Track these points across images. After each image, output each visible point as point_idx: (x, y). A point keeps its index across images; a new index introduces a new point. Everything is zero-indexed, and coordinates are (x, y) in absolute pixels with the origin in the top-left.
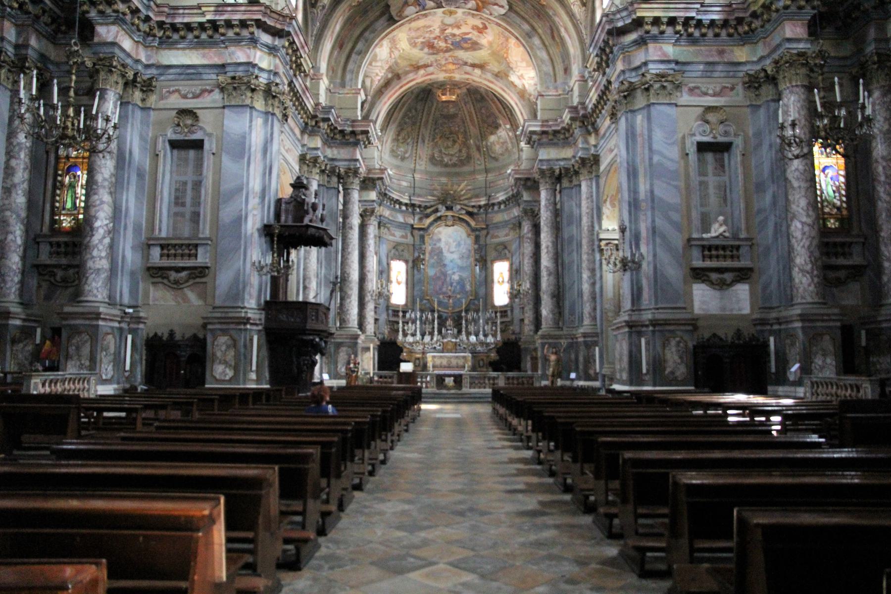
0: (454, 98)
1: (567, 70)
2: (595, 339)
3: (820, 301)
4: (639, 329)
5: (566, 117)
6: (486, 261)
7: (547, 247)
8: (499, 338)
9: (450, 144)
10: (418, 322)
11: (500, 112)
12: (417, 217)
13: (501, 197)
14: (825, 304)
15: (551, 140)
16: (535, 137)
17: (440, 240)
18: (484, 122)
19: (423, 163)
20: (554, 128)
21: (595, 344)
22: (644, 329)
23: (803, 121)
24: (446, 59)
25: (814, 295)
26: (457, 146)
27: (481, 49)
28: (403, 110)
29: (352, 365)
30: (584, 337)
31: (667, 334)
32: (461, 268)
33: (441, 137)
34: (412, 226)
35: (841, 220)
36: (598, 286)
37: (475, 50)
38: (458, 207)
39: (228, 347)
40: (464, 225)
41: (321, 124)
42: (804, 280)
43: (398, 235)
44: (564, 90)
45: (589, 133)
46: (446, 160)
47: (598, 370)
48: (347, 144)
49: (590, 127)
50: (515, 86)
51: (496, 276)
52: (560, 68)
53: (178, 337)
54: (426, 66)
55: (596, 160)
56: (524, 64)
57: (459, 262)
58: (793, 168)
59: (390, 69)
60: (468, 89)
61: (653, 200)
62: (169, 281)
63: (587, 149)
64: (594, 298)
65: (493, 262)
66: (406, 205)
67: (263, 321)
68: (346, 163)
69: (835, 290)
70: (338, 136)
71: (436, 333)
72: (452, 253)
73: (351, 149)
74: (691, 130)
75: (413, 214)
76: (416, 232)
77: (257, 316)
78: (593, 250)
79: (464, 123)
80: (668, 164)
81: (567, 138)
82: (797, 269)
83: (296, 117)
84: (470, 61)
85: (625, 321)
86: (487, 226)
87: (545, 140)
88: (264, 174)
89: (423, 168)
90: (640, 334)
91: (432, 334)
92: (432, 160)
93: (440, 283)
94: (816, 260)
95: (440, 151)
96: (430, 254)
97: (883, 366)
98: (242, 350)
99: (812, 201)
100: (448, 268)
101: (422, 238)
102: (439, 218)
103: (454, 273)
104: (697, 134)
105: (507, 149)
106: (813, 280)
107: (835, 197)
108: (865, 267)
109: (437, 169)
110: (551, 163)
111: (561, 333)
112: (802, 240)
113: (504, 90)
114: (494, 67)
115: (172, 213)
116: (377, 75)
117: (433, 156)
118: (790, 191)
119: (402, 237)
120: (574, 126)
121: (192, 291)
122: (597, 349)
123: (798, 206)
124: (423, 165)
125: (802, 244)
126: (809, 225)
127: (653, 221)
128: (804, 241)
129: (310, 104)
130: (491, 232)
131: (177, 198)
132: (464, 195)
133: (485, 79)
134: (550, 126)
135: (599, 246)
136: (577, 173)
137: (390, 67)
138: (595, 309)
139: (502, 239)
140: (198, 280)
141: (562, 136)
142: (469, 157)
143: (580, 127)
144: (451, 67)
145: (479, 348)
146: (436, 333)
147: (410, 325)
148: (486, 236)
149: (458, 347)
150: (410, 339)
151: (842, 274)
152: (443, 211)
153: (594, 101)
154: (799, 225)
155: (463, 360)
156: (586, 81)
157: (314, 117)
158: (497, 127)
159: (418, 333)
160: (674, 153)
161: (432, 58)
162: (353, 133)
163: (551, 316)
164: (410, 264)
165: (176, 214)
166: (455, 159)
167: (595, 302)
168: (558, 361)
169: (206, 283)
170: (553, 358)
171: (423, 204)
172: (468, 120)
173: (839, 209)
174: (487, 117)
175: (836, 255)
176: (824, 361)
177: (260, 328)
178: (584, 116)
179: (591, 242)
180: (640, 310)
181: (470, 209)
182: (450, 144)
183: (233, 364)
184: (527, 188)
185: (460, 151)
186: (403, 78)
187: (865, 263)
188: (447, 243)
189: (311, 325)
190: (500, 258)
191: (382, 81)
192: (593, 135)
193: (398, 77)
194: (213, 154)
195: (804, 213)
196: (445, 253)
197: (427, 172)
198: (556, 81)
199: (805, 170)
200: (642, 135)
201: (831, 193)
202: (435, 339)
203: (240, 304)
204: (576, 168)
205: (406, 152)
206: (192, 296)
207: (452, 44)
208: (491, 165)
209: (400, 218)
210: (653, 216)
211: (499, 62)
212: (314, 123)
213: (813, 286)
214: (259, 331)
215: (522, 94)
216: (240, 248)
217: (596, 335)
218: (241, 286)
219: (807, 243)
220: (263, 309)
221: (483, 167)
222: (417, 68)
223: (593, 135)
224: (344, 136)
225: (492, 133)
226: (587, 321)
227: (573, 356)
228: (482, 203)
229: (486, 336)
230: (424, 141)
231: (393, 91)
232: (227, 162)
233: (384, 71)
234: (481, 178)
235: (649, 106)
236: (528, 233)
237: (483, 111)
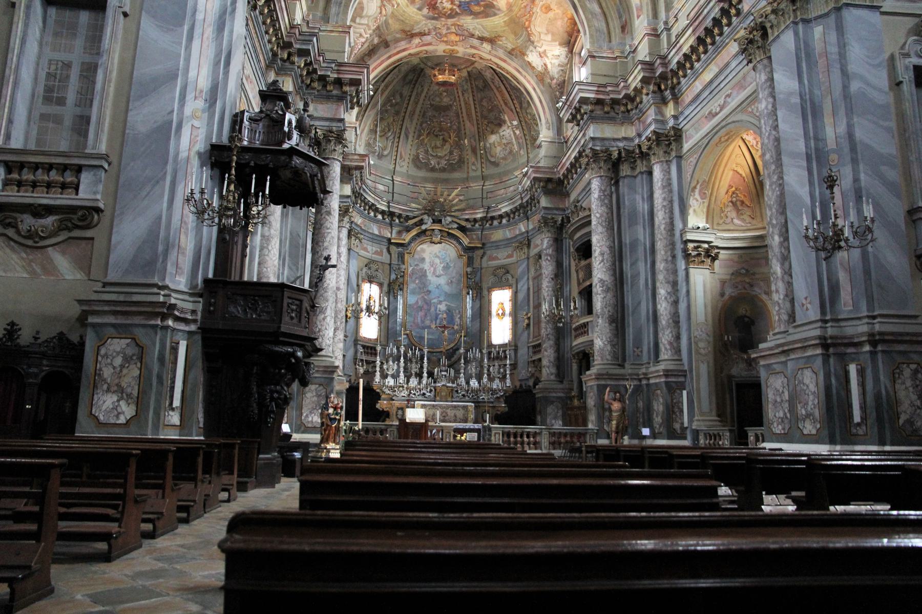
0: (453, 79)
1: (626, 27)
2: (682, 379)
4: (842, 349)
5: (635, 79)
6: (481, 288)
7: (602, 254)
8: (508, 383)
9: (439, 143)
10: (402, 360)
11: (506, 104)
12: (395, 230)
13: (505, 208)
15: (608, 113)
16: (585, 108)
17: (423, 260)
18: (485, 118)
19: (405, 164)
20: (612, 96)
21: (682, 386)
22: (851, 350)
24: (448, 29)
26: (447, 147)
27: (495, 15)
28: (386, 93)
29: (331, 411)
30: (666, 376)
31: (899, 359)
32: (448, 296)
33: (428, 134)
34: (389, 240)
36: (682, 306)
37: (487, 15)
38: (449, 219)
39: (127, 360)
40: (455, 242)
41: (296, 59)
43: (370, 250)
44: (622, 52)
45: (664, 102)
46: (432, 162)
47: (686, 425)
48: (328, 98)
49: (667, 93)
50: (533, 68)
51: (494, 308)
52: (615, 25)
53: (25, 337)
54: (421, 34)
55: (677, 135)
56: (549, 37)
57: (447, 288)
59: (378, 31)
60: (468, 72)
61: (853, 149)
62: (18, 232)
63: (663, 122)
64: (676, 322)
65: (490, 290)
66: (383, 213)
67: (199, 317)
68: (327, 124)
70: (316, 85)
71: (425, 375)
72: (437, 276)
73: (334, 106)
74: (903, 47)
75: (391, 225)
76: (394, 249)
77: (190, 306)
78: (674, 257)
79: (458, 116)
80: (875, 94)
81: (628, 111)
83: (263, 38)
84: (477, 33)
85: (820, 337)
86: (484, 244)
87: (598, 112)
88: (217, 64)
89: (404, 170)
90: (844, 359)
91: (419, 375)
92: (416, 162)
93: (421, 314)
95: (427, 152)
98: (156, 368)
100: (432, 296)
101: (401, 257)
103: (440, 302)
104: (912, 54)
105: (511, 152)
109: (422, 174)
110: (607, 143)
111: (622, 371)
113: (519, 72)
114: (508, 42)
115: (36, 114)
116: (361, 35)
117: (417, 157)
119: (376, 253)
120: (644, 91)
121: (63, 253)
122: (685, 392)
124: (404, 166)
127: (856, 180)
129: (284, 22)
130: (488, 253)
131: (49, 90)
132: (456, 205)
133: (495, 56)
134: (608, 93)
135: (685, 250)
136: (644, 156)
137: (378, 28)
138: (678, 337)
140: (77, 233)
141: (622, 108)
142: (461, 161)
143: (654, 92)
144: (453, 38)
145: (483, 396)
146: (425, 375)
147: (391, 363)
148: (482, 258)
149: (455, 395)
150: (390, 381)
152: (428, 224)
153: (686, 49)
156: (658, 36)
157: (288, 45)
158: (500, 123)
159: (402, 374)
160: (881, 79)
161: (431, 24)
162: (339, 82)
163: (609, 348)
164: (385, 288)
165: (44, 117)
166: (443, 162)
167: (679, 328)
168: (623, 410)
169: (92, 239)
170: (616, 406)
171: (404, 214)
172: (465, 114)
174: (491, 111)
177: (193, 327)
178: (663, 77)
179: (672, 244)
180: (838, 320)
181: (463, 223)
182: (439, 143)
183: (135, 393)
184: (547, 192)
185: (451, 153)
186: (392, 47)
188: (432, 264)
189: (288, 326)
190: (501, 284)
191: (366, 45)
192: (671, 105)
193: (386, 44)
194: (125, 15)
196: (430, 276)
197: (409, 176)
198: (610, 41)
200: (826, 54)
202: (424, 381)
203: (156, 280)
204: (644, 149)
205: (384, 149)
206: (62, 262)
207: (459, 6)
208: (492, 170)
210: (856, 172)
211: (515, 34)
212: (286, 56)
214: (190, 333)
215: (541, 77)
216: (163, 178)
217: (683, 374)
218: (161, 248)
220: (201, 296)
221: (479, 173)
222: (410, 35)
223: (671, 105)
224: (325, 86)
225: (492, 133)
226: (665, 354)
227: (641, 404)
228: (479, 216)
229: (491, 379)
230: (407, 137)
231: (379, 61)
232: (149, 28)
233: (371, 31)
234: (476, 186)
235: (838, 9)
236: (547, 248)
237: (485, 104)
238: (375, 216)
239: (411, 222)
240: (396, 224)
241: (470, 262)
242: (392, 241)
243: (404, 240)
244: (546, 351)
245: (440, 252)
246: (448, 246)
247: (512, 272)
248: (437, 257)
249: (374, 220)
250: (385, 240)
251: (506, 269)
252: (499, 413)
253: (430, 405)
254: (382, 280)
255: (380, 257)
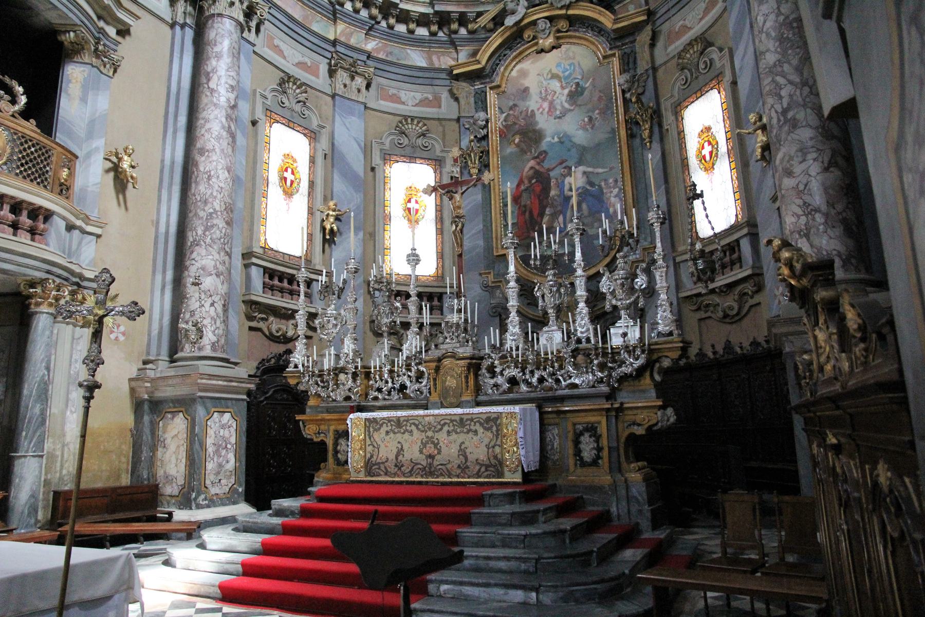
17: (526, 90)
34: (449, 71)
40: (589, 35)
57: (581, 137)
66: (423, 20)
75: (453, 44)
96: (502, 135)
102: (516, 37)
119: (423, 103)
130: (665, 28)
139: (697, 30)
148: (652, 45)
155: (485, 436)
196: (544, 122)
209: (417, 58)
238: (411, 32)
239: (483, 21)
240: (463, 39)
241: (629, 62)
242: (455, 72)
243: (479, 62)
244: (789, 173)
245: (558, 65)
246: (573, 48)
247: (719, 42)
248: (554, 76)
249: (411, 40)
250: (444, 76)
251: (704, 42)
252: (640, 431)
253: (389, 420)
254: (438, 153)
255: (435, 110)
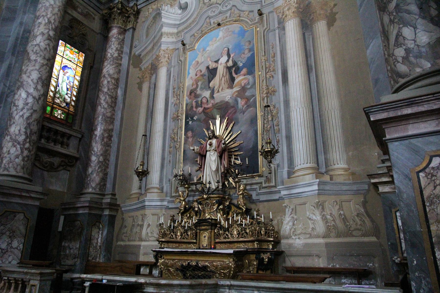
3: (26, 176)
14: (30, 181)
23: (56, 10)
25: (19, 168)
35: (68, 114)
42: (13, 150)
58: (35, 43)
69: (45, 173)
82: (8, 138)
94: (32, 133)
97: (72, 251)
99: (44, 77)
106: (22, 152)
107: (67, 94)
108: (77, 159)
112: (23, 108)
118: (26, 61)
123: (29, 77)
125: (21, 113)
126: (34, 98)
128: (25, 111)
151: (56, 161)
154: (24, 95)
173: (67, 104)
175: (55, 142)
176: (9, 244)
187: (77, 156)
195: (33, 86)
199: (46, 48)
201: (65, 89)
213: (21, 158)
219: (27, 115)
